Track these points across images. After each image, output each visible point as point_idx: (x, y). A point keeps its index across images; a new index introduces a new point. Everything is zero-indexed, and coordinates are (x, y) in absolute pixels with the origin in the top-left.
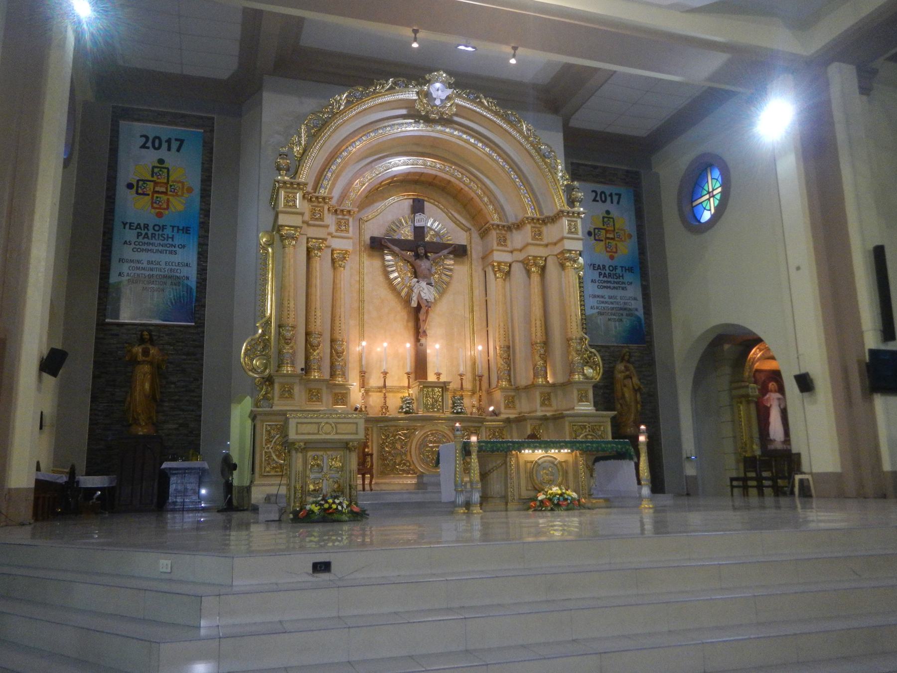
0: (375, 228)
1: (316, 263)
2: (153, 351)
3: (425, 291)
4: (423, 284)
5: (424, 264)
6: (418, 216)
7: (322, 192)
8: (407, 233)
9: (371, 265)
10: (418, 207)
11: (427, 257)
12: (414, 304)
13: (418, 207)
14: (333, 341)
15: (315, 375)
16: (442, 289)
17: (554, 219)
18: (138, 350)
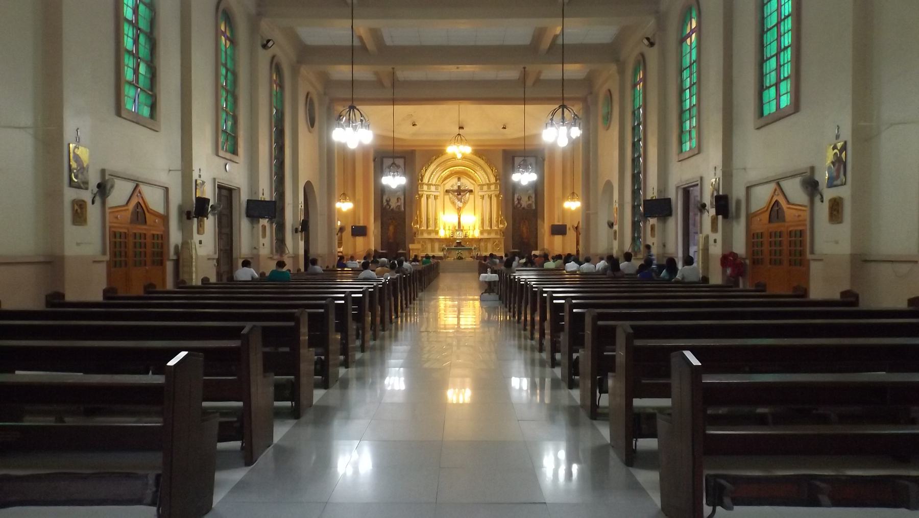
0: (448, 187)
1: (430, 200)
2: (394, 222)
3: (460, 205)
4: (459, 202)
5: (460, 197)
6: (459, 182)
7: (430, 183)
8: (456, 188)
9: (447, 197)
10: (459, 179)
11: (460, 194)
12: (457, 207)
13: (459, 179)
14: (436, 219)
15: (430, 229)
16: (465, 203)
17: (491, 184)
18: (390, 221)
